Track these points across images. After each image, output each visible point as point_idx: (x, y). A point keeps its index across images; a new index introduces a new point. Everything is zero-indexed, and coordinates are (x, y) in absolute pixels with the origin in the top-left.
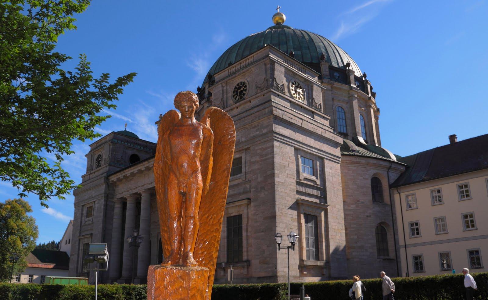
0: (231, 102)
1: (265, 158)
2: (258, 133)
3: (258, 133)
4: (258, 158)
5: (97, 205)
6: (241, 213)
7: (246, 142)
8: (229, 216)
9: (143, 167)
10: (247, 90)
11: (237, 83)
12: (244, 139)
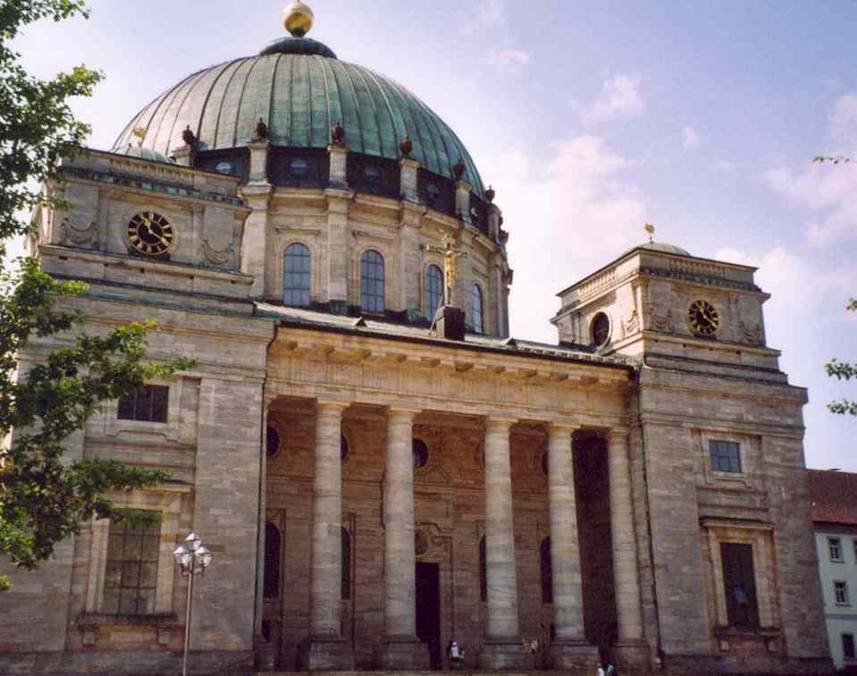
0: (685, 327)
1: (792, 464)
2: (778, 419)
3: (778, 419)
4: (778, 461)
5: (212, 392)
6: (750, 542)
7: (757, 424)
8: (722, 541)
9: (451, 358)
10: (720, 324)
11: (698, 299)
12: (751, 418)
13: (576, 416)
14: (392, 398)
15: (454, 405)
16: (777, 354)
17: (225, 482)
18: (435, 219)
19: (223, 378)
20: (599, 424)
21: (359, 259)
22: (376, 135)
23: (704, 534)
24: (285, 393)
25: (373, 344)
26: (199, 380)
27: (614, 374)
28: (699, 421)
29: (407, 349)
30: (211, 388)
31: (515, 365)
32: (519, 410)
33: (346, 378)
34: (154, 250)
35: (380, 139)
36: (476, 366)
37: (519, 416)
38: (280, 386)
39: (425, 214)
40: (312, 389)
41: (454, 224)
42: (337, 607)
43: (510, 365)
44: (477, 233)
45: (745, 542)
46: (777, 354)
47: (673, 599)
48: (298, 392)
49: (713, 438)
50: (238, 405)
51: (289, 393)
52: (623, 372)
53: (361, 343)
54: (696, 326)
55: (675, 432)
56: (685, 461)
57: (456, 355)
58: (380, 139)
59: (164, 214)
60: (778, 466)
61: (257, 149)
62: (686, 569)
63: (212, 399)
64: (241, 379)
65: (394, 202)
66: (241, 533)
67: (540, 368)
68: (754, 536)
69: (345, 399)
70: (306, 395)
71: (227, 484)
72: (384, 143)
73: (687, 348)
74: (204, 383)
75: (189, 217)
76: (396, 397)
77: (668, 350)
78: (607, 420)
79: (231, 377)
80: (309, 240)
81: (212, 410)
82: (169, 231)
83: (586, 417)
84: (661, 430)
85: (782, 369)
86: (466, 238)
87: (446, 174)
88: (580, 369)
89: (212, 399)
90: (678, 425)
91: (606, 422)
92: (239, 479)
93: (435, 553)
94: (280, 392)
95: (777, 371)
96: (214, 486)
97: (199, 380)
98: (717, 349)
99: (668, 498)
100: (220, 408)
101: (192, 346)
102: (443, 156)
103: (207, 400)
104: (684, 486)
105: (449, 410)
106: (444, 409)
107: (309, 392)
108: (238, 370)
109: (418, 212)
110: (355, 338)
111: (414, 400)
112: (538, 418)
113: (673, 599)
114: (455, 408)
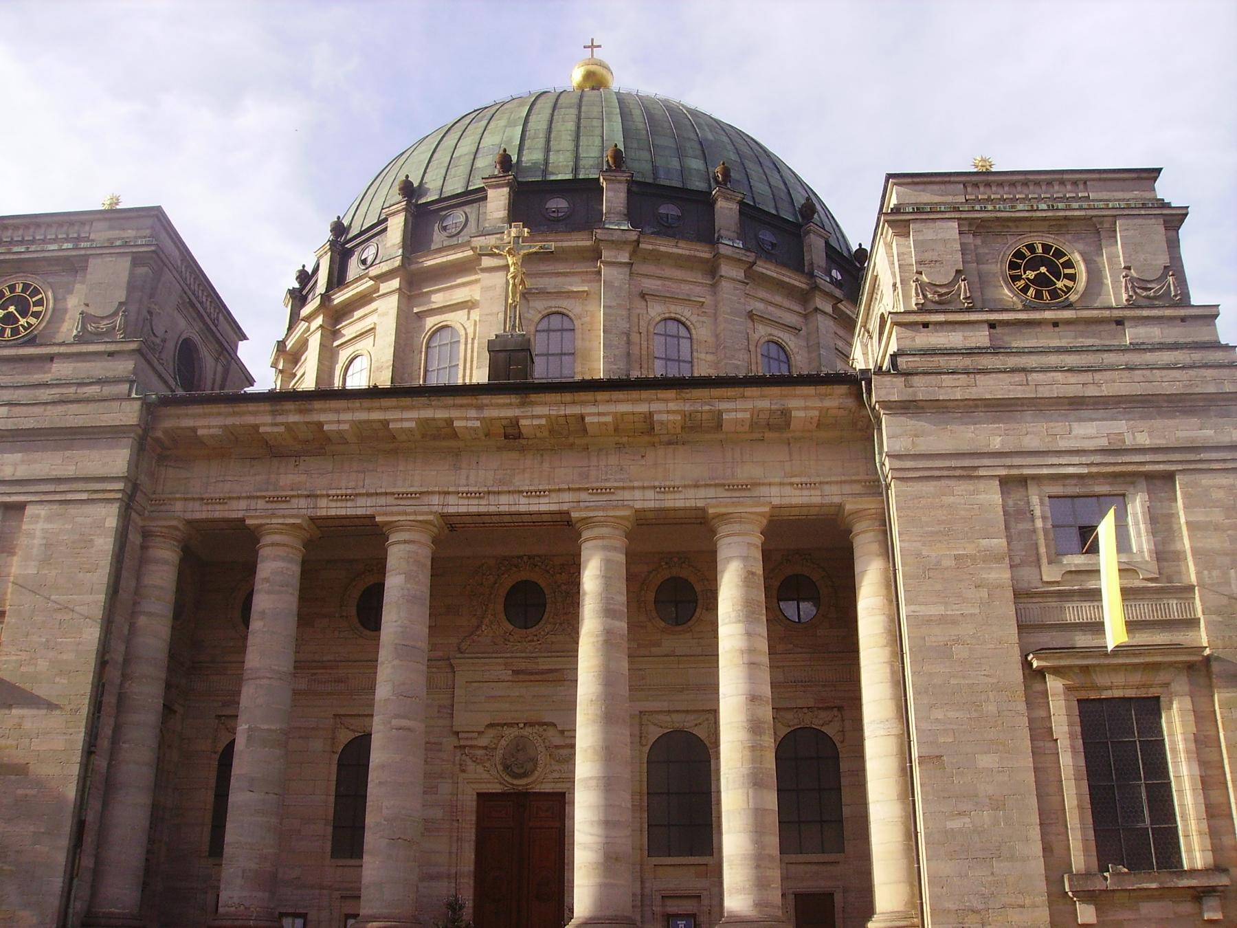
6: (1153, 692)
8: (1084, 695)
9: (473, 413)
12: (1143, 440)
13: (764, 491)
14: (382, 501)
15: (504, 499)
16: (1209, 315)
17: (40, 662)
18: (662, 249)
19: (58, 497)
20: (816, 500)
21: (532, 329)
22: (568, 154)
23: (1038, 687)
24: (198, 516)
25: (324, 411)
26: (21, 507)
27: (822, 397)
28: (1017, 461)
29: (386, 409)
30: (38, 516)
31: (602, 408)
32: (638, 494)
33: (304, 477)
34: (15, 331)
35: (577, 158)
36: (523, 422)
37: (638, 505)
38: (190, 505)
39: (638, 242)
40: (243, 504)
41: (704, 252)
42: (254, 866)
43: (593, 409)
44: (751, 260)
45: (1142, 693)
46: (1209, 315)
47: (955, 824)
48: (219, 512)
49: (1057, 489)
50: (76, 537)
51: (204, 516)
52: (842, 389)
53: (301, 412)
54: (1025, 290)
55: (961, 487)
56: (984, 542)
57: (480, 408)
58: (577, 158)
59: (35, 282)
60: (1217, 528)
61: (394, 214)
62: (986, 761)
63: (38, 534)
64: (84, 496)
65: (585, 235)
66: (58, 743)
67: (655, 407)
68: (1162, 677)
69: (300, 510)
70: (234, 515)
71: (42, 665)
72: (582, 163)
73: (999, 330)
74: (30, 510)
75: (71, 279)
76: (390, 500)
77: (954, 339)
78: (834, 489)
79: (69, 497)
80: (456, 319)
81: (35, 551)
82: (40, 303)
83: (788, 490)
84: (929, 487)
85: (1223, 342)
86: (726, 270)
87: (698, 184)
88: (743, 397)
89: (38, 534)
90: (969, 475)
91: (832, 495)
92: (64, 657)
93: (556, 775)
94: (189, 516)
95: (1216, 346)
96: (23, 669)
97: (21, 507)
98: (1069, 322)
99: (942, 620)
100: (48, 546)
101: (18, 456)
102: (696, 164)
103: (31, 535)
104: (984, 593)
105: (492, 509)
106: (483, 509)
107: (236, 510)
108: (81, 486)
109: (625, 242)
110: (290, 406)
111: (426, 499)
112: (680, 504)
113: (955, 824)
114: (503, 504)
